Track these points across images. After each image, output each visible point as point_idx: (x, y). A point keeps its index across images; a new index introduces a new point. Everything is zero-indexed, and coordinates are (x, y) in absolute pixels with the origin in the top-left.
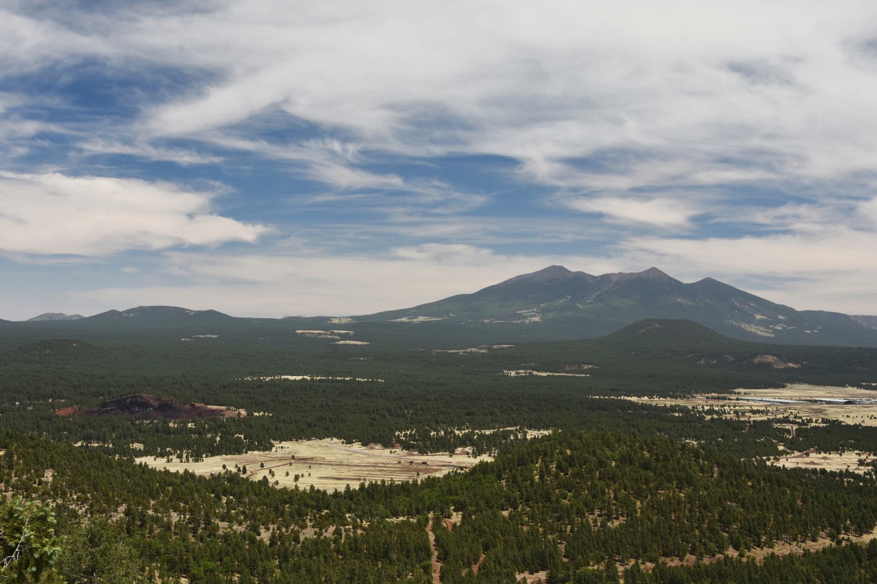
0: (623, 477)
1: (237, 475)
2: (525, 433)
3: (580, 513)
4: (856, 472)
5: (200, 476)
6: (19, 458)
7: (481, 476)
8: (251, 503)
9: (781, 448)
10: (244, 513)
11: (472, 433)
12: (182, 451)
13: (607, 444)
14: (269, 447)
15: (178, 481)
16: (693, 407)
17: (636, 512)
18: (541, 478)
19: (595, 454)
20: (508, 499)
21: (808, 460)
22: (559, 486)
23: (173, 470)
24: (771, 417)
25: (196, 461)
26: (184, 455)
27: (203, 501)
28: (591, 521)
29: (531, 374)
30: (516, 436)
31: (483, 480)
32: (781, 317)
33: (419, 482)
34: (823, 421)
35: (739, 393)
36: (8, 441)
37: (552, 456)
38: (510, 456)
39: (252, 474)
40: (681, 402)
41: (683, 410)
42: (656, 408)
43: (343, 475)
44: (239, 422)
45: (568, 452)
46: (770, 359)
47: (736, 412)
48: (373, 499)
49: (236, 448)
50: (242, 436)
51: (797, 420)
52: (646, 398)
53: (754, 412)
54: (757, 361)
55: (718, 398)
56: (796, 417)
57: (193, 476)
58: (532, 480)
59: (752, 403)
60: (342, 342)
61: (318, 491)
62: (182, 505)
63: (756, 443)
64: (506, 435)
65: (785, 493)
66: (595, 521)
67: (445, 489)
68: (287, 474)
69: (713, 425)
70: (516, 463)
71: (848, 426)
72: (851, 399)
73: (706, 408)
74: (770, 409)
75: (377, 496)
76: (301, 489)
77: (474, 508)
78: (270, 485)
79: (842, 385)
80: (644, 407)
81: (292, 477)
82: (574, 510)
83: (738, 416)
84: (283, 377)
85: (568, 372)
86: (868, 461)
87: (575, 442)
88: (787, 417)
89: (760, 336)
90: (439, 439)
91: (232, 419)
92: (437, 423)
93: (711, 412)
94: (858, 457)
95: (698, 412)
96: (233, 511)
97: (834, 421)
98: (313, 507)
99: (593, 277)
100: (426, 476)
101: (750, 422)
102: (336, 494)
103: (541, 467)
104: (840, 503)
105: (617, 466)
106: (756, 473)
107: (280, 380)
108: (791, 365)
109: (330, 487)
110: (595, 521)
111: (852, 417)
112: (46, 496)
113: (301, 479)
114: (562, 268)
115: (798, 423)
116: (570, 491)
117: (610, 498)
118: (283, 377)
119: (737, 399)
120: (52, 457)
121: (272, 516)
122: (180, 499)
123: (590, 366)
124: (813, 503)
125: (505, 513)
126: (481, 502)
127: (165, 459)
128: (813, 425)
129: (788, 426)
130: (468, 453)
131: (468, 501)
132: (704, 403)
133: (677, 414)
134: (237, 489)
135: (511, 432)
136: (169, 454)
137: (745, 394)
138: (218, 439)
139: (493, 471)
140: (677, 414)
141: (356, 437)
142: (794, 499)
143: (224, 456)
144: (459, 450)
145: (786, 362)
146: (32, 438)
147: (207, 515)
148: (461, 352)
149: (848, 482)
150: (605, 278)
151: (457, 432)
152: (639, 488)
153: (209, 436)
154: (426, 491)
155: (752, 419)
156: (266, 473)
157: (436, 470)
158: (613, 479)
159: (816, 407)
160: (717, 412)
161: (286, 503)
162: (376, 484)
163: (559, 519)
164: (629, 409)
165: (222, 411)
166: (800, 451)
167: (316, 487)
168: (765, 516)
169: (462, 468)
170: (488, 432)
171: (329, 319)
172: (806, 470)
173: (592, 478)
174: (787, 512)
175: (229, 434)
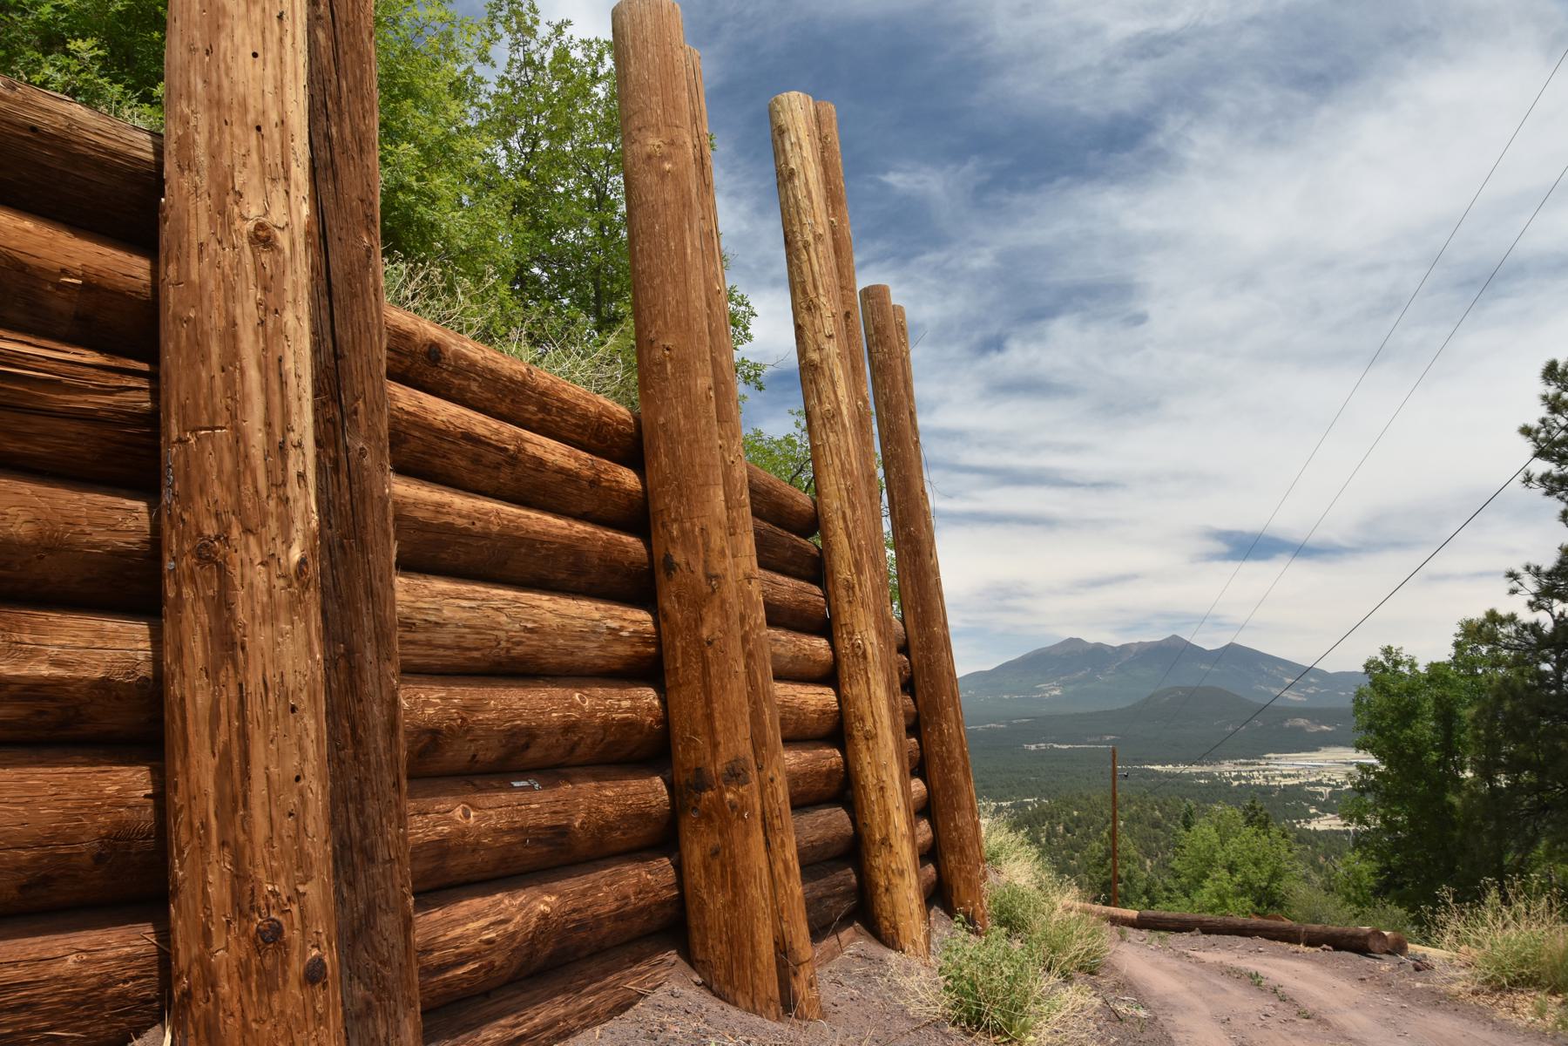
9: (1313, 811)
16: (1220, 774)
24: (1303, 780)
32: (1312, 680)
35: (1269, 758)
40: (1206, 769)
41: (1209, 776)
42: (1180, 775)
46: (1302, 722)
51: (1331, 783)
52: (1170, 766)
53: (1284, 776)
54: (1287, 725)
55: (1247, 764)
56: (1329, 780)
59: (1283, 767)
69: (1239, 790)
73: (1233, 774)
74: (1301, 772)
80: (1168, 775)
83: (1267, 781)
85: (1090, 744)
89: (1290, 700)
93: (1238, 778)
95: (1225, 778)
99: (1112, 647)
101: (1280, 786)
108: (1324, 727)
114: (1079, 640)
115: (1332, 786)
119: (1267, 764)
129: (1320, 789)
132: (1232, 769)
133: (1202, 781)
135: (1028, 803)
140: (1202, 781)
145: (1319, 724)
148: (980, 728)
150: (1124, 648)
155: (1282, 784)
160: (1244, 778)
164: (1152, 777)
166: (1333, 813)
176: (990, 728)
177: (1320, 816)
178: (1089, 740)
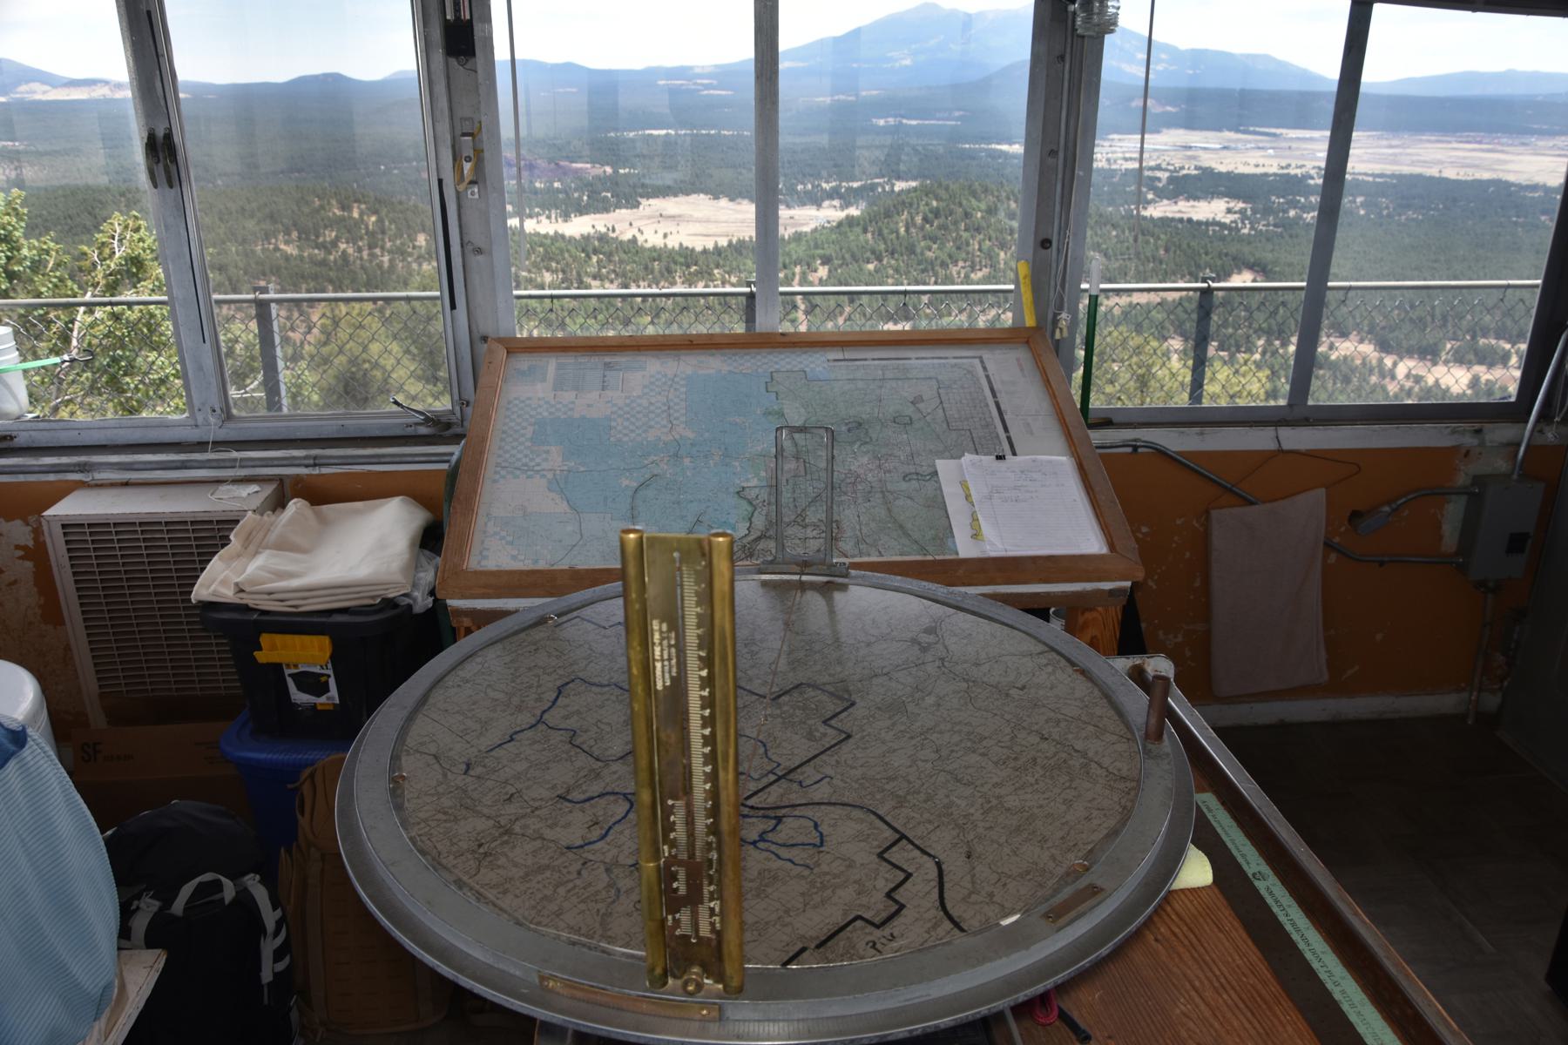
0: (988, 227)
1: (606, 234)
2: (893, 185)
3: (944, 265)
4: (1223, 220)
5: (570, 237)
6: (390, 223)
7: (848, 229)
8: (621, 262)
9: (1150, 196)
10: (614, 271)
11: (840, 186)
12: (550, 211)
13: (974, 194)
14: (637, 205)
15: (548, 242)
17: (999, 263)
18: (907, 230)
19: (960, 204)
20: (873, 252)
21: (1175, 208)
22: (924, 238)
23: (543, 231)
25: (566, 221)
26: (553, 216)
27: (574, 261)
28: (954, 273)
29: (900, 122)
30: (884, 188)
31: (849, 234)
33: (786, 237)
34: (1196, 168)
35: (1113, 140)
36: (377, 206)
37: (918, 207)
38: (875, 208)
39: (622, 233)
43: (711, 232)
44: (602, 179)
45: (935, 203)
47: (1108, 160)
48: (741, 254)
49: (605, 207)
50: (609, 195)
53: (1126, 159)
56: (1168, 164)
57: (563, 237)
58: (897, 232)
60: (706, 92)
61: (687, 248)
62: (554, 265)
63: (1125, 192)
64: (873, 187)
65: (1147, 242)
66: (959, 273)
67: (812, 244)
68: (656, 232)
70: (882, 216)
71: (1220, 174)
72: (1226, 144)
75: (744, 252)
76: (670, 246)
77: (840, 262)
78: (639, 243)
79: (1219, 129)
81: (660, 235)
82: (939, 262)
84: (647, 132)
85: (938, 119)
86: (1237, 209)
87: (942, 193)
88: (1159, 165)
90: (806, 192)
91: (598, 178)
92: (804, 175)
94: (1227, 205)
96: (604, 270)
97: (1207, 168)
98: (681, 264)
100: (793, 230)
102: (705, 251)
103: (906, 220)
104: (1202, 251)
105: (983, 217)
106: (1121, 223)
107: (644, 135)
108: (1169, 108)
109: (698, 245)
110: (959, 273)
111: (1225, 164)
112: (421, 260)
113: (669, 237)
116: (935, 243)
117: (974, 249)
118: (647, 132)
119: (1111, 146)
120: (422, 221)
121: (642, 274)
122: (551, 259)
123: (961, 113)
124: (1175, 252)
125: (871, 267)
126: (847, 256)
127: (535, 220)
128: (1185, 172)
129: (1159, 174)
130: (835, 207)
131: (834, 255)
134: (606, 248)
135: (879, 184)
136: (538, 215)
137: (1120, 140)
138: (585, 198)
139: (858, 224)
141: (722, 193)
142: (1157, 249)
143: (593, 215)
144: (826, 203)
146: (401, 203)
147: (579, 274)
149: (1213, 230)
151: (824, 185)
152: (1004, 239)
153: (576, 195)
154: (793, 245)
155: (1123, 167)
156: (634, 231)
157: (803, 225)
158: (978, 230)
159: (1189, 153)
161: (655, 260)
162: (744, 241)
163: (923, 271)
164: (1000, 157)
165: (587, 169)
167: (685, 245)
168: (1126, 266)
169: (829, 222)
170: (855, 185)
171: (691, 68)
172: (1173, 219)
173: (957, 230)
174: (1149, 261)
175: (595, 192)
176: (838, 100)
177: (1156, 202)
178: (938, 115)
